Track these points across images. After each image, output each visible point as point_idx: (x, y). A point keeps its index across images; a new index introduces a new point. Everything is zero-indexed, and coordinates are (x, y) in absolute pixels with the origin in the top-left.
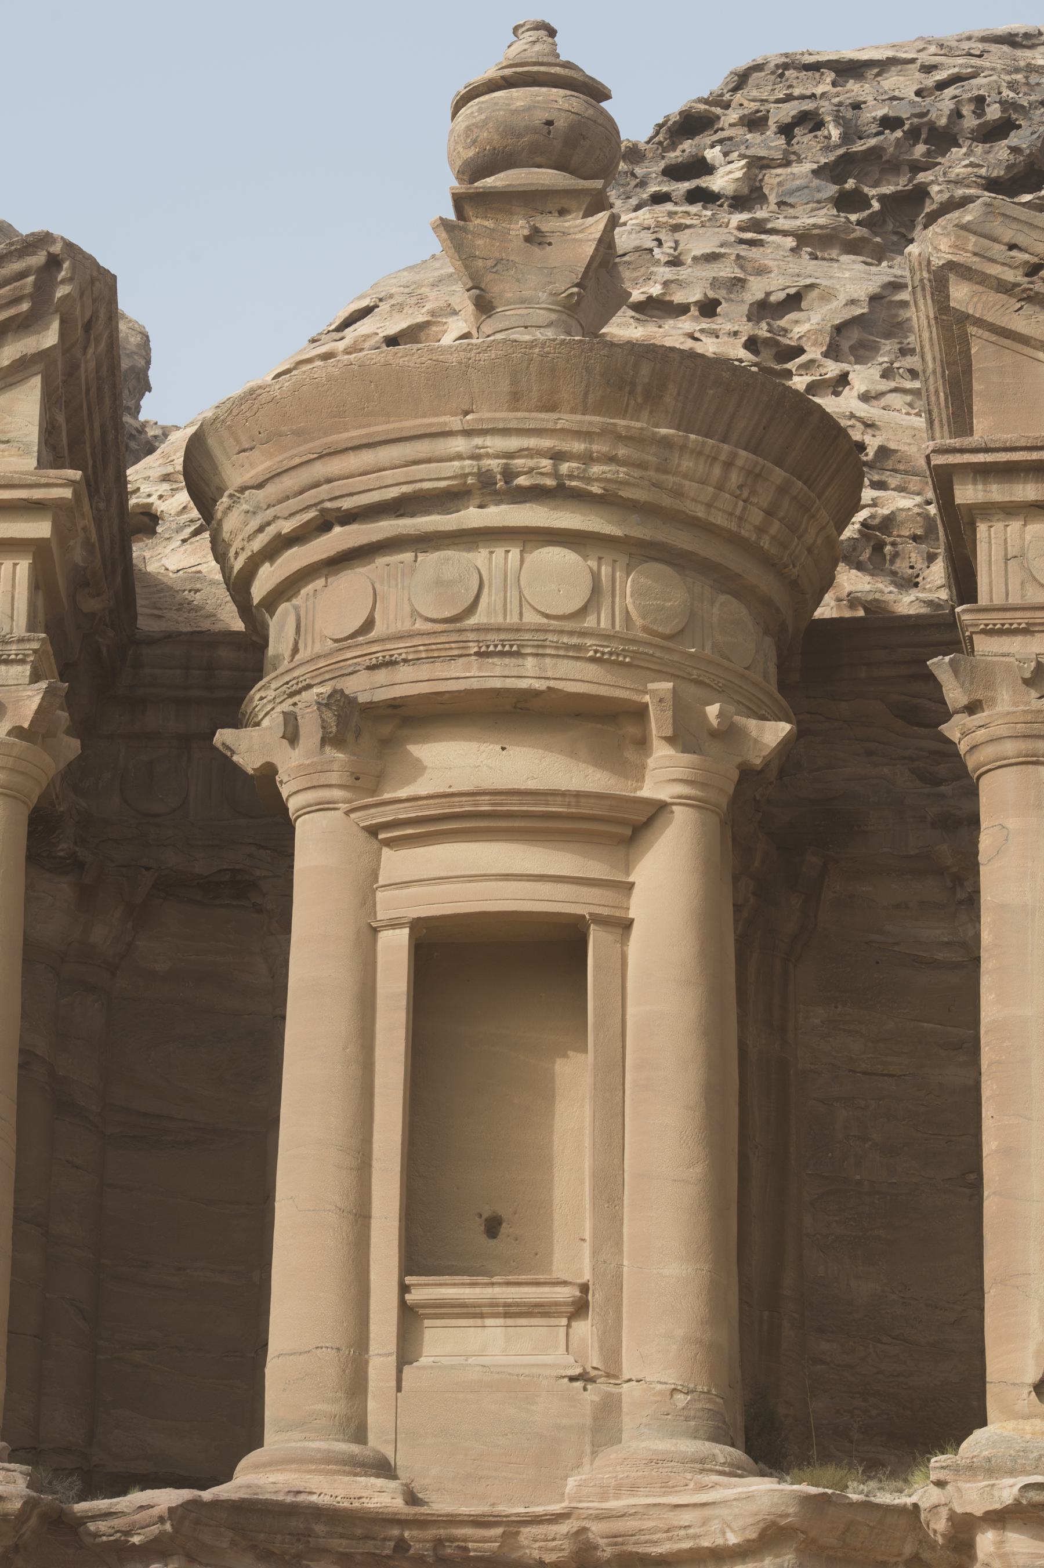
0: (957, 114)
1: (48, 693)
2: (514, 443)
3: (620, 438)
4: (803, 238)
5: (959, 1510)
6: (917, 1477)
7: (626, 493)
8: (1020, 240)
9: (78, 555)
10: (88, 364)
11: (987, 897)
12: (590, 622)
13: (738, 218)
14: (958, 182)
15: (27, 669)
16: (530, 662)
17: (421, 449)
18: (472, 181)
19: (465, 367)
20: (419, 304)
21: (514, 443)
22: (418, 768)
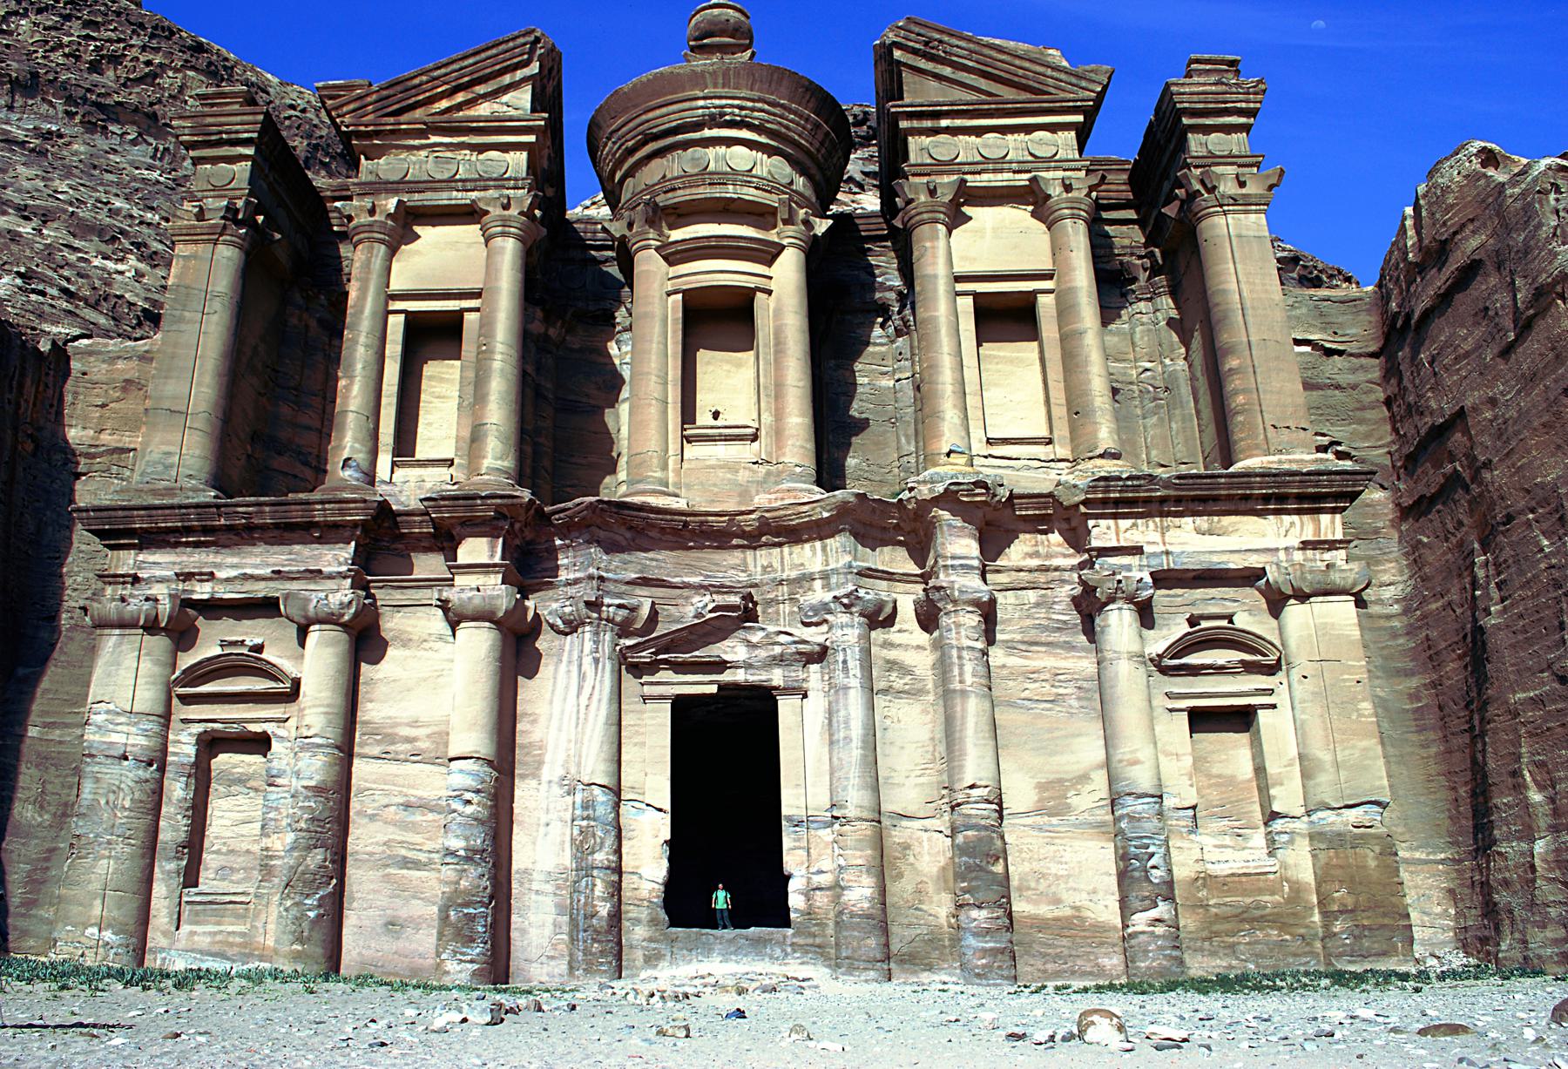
1: (535, 196)
2: (724, 102)
8: (922, 31)
10: (550, 89)
16: (731, 187)
21: (724, 102)
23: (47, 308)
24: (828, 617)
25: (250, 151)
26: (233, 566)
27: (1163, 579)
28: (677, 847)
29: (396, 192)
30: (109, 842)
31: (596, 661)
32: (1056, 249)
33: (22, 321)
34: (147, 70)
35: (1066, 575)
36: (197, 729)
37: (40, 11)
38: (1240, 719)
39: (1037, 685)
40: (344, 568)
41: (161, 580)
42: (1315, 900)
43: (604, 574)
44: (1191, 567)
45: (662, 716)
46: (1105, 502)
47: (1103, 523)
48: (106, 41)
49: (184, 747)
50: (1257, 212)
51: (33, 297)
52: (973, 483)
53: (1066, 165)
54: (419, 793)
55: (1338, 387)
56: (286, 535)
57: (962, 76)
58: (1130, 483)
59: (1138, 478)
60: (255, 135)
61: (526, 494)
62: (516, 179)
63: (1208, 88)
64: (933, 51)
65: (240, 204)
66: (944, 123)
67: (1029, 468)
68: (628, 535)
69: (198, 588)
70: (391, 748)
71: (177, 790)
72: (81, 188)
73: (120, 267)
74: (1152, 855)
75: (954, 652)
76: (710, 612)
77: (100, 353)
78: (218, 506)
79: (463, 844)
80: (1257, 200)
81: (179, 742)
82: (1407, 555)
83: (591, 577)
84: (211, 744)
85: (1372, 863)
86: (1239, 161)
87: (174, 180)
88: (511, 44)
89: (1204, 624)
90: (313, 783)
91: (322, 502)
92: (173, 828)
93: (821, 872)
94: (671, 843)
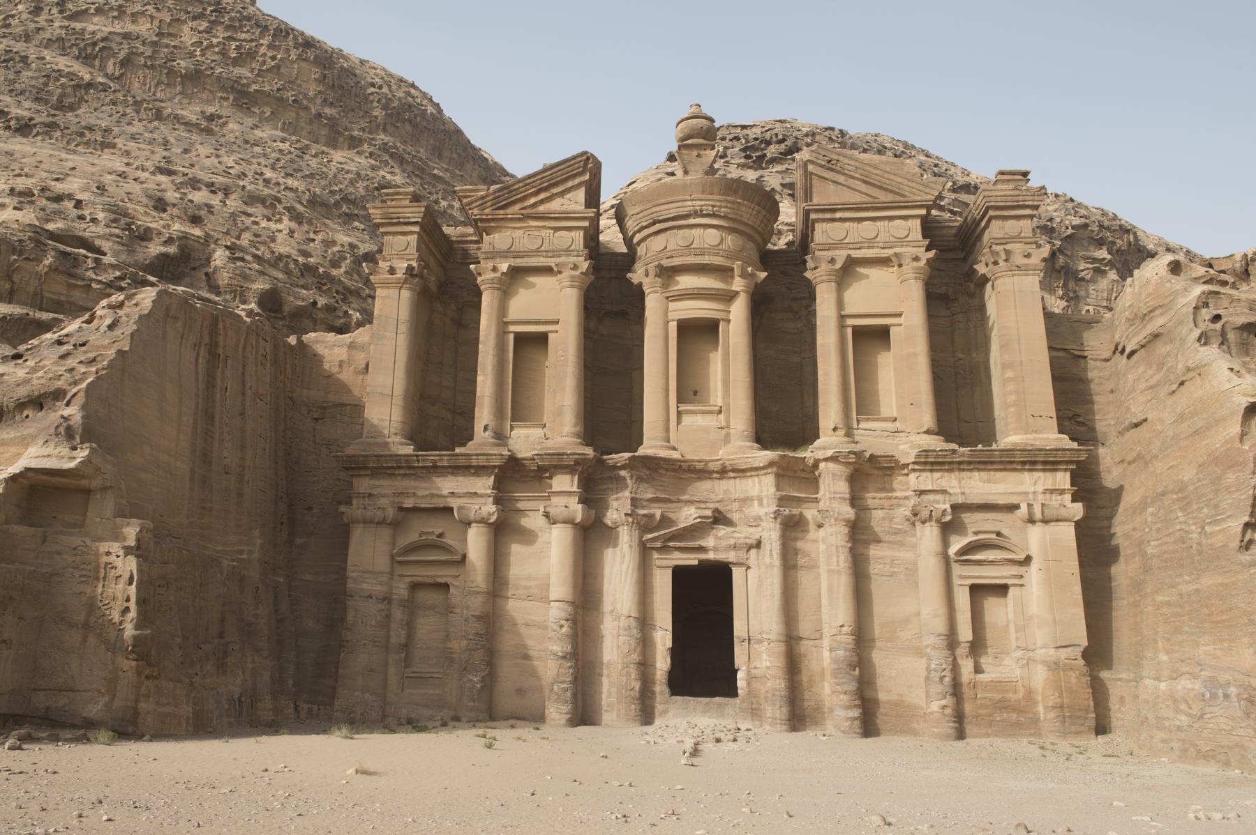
0: (771, 138)
2: (703, 203)
3: (728, 202)
4: (739, 165)
5: (817, 458)
6: (806, 450)
7: (730, 216)
8: (826, 154)
9: (592, 232)
10: (594, 185)
11: (818, 314)
12: (720, 247)
13: (722, 161)
14: (773, 153)
17: (680, 204)
18: (682, 141)
19: (691, 184)
20: (648, 179)
21: (703, 203)
22: (678, 283)
23: (248, 271)
24: (761, 523)
25: (417, 229)
26: (426, 489)
27: (956, 508)
28: (675, 652)
29: (506, 257)
30: (364, 645)
31: (631, 546)
33: (234, 282)
34: (273, 63)
36: (408, 580)
37: (194, 18)
39: (881, 566)
40: (489, 491)
41: (384, 496)
43: (634, 495)
44: (975, 502)
46: (925, 463)
48: (243, 41)
49: (401, 590)
50: (1034, 275)
51: (239, 264)
52: (850, 452)
53: (912, 244)
54: (533, 618)
56: (455, 471)
57: (851, 182)
58: (940, 453)
59: (946, 451)
60: (420, 220)
61: (589, 452)
62: (578, 251)
64: (833, 167)
65: (415, 264)
66: (838, 215)
68: (648, 472)
69: (406, 501)
70: (515, 593)
71: (398, 614)
72: (242, 162)
73: (280, 226)
74: (944, 670)
76: (695, 519)
77: (323, 342)
78: (417, 456)
79: (559, 649)
80: (1033, 268)
81: (398, 587)
84: (415, 586)
85: (1074, 681)
87: (300, 149)
88: (573, 162)
89: (981, 537)
90: (476, 613)
91: (477, 455)
92: (397, 636)
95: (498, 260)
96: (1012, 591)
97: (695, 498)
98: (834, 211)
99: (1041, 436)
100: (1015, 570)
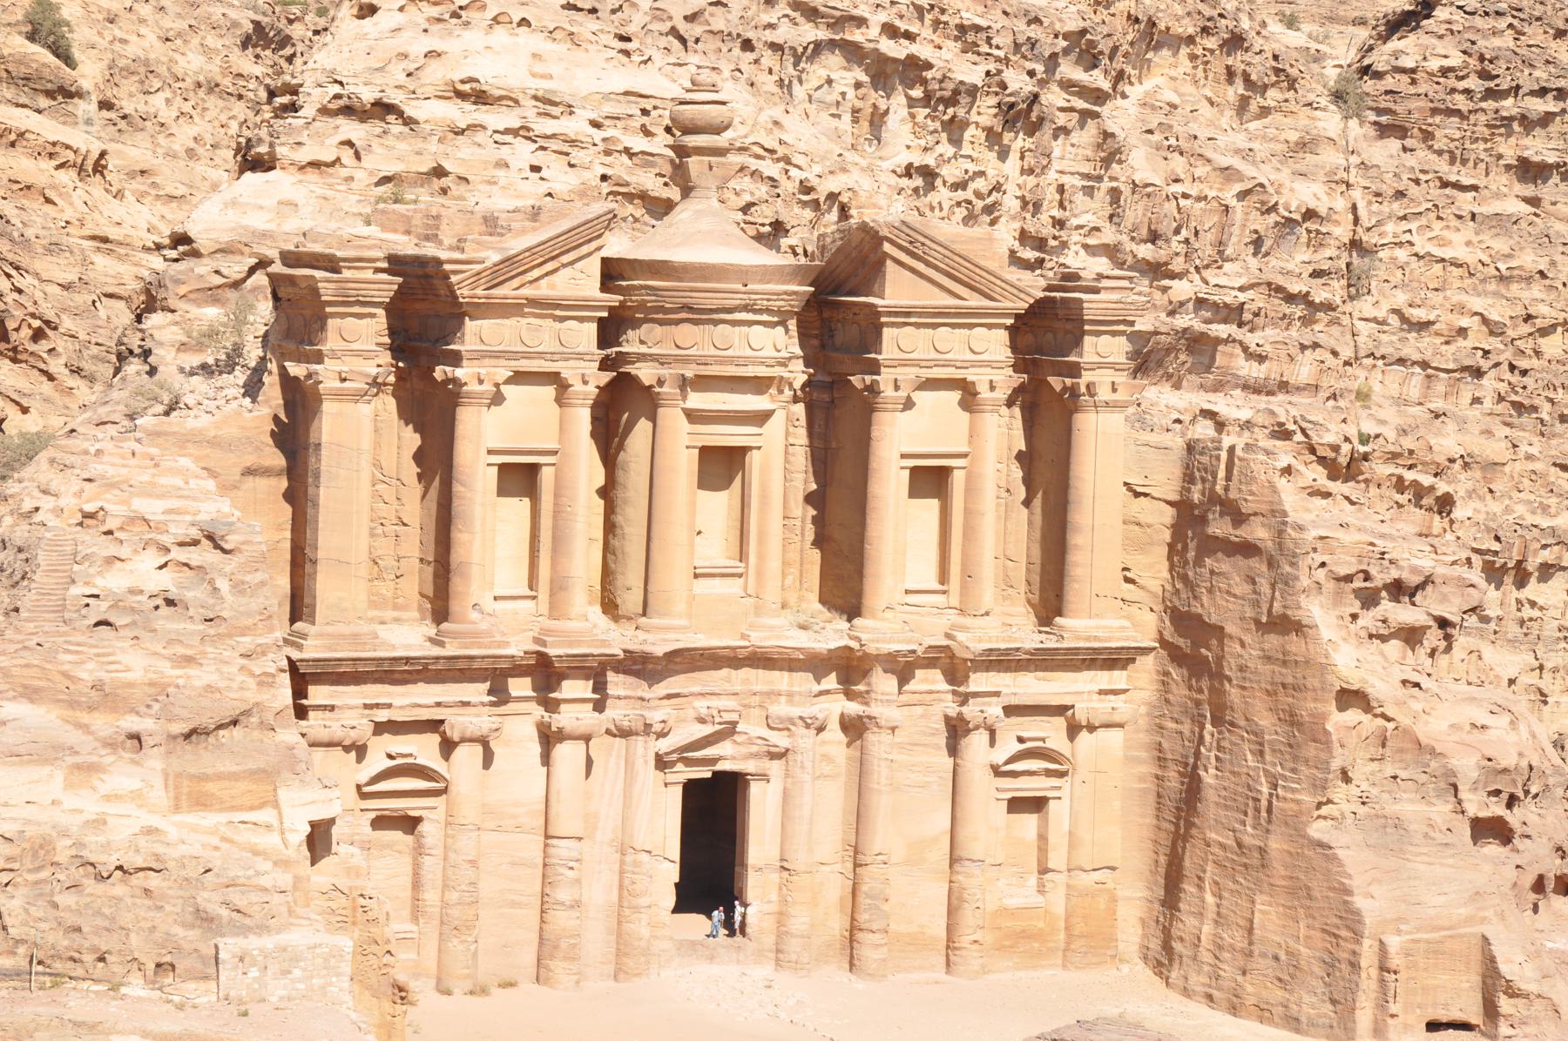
8: (911, 233)
15: (597, 364)
27: (1010, 711)
32: (972, 435)
35: (943, 696)
36: (373, 815)
38: (1036, 804)
42: (1062, 924)
45: (676, 794)
47: (979, 674)
53: (994, 365)
55: (1138, 524)
63: (1114, 306)
66: (913, 320)
67: (930, 614)
75: (876, 761)
76: (720, 723)
77: (166, 434)
82: (1158, 672)
83: (642, 699)
86: (1117, 367)
89: (1029, 745)
90: (470, 858)
93: (770, 902)
94: (677, 885)
95: (487, 361)
96: (1052, 804)
97: (707, 689)
98: (908, 314)
99: (1103, 622)
100: (1054, 782)
